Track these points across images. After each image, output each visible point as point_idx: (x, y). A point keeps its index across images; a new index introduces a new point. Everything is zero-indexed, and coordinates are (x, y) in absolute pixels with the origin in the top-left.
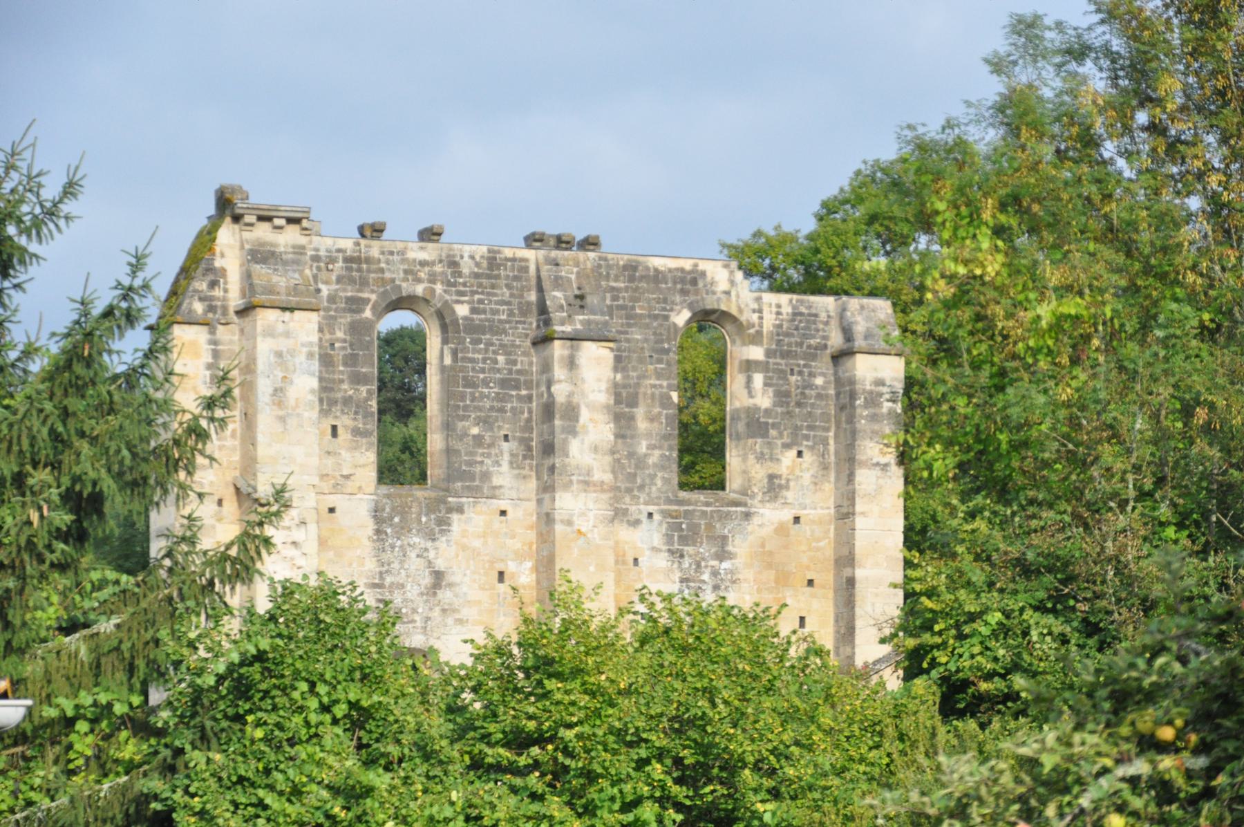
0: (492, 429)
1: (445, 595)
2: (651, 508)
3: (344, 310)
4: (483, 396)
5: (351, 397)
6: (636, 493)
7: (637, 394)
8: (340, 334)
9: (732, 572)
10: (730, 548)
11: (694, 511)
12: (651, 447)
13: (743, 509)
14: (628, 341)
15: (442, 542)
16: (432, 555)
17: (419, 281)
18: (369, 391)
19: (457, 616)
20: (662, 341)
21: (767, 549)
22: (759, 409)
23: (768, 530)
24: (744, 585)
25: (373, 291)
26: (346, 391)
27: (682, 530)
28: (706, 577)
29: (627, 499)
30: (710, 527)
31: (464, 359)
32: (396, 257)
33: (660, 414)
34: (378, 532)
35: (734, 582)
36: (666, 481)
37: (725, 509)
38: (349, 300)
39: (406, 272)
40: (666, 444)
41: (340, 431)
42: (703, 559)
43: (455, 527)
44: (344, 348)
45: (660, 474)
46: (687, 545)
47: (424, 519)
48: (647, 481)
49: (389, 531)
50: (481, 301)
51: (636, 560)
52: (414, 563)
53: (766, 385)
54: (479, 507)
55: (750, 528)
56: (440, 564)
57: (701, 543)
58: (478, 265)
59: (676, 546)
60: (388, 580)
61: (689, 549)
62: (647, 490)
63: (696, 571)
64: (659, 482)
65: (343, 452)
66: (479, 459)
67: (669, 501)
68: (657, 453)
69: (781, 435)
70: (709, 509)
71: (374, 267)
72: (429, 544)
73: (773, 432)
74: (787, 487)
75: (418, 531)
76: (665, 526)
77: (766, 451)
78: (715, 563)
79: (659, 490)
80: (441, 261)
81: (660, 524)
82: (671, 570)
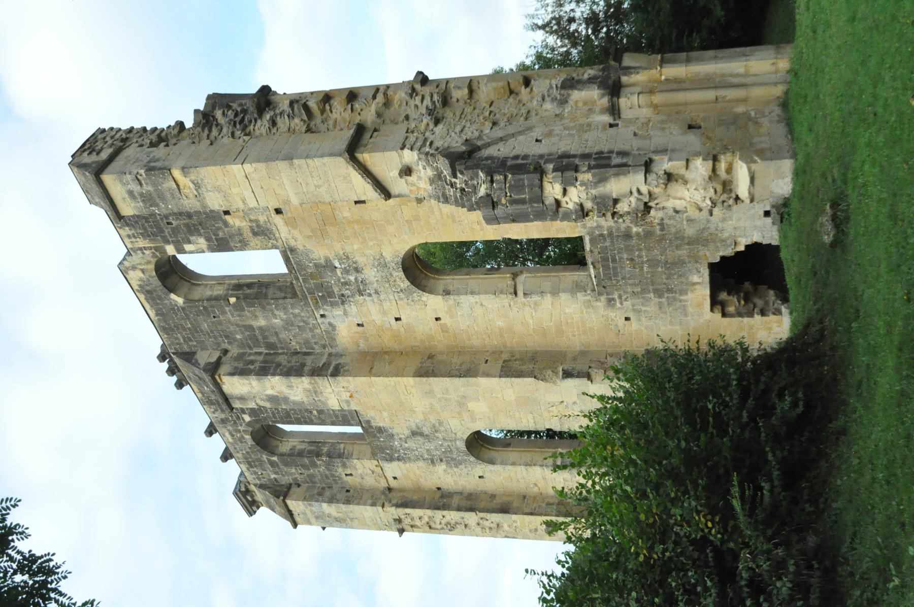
1: (426, 430)
2: (318, 316)
3: (279, 468)
6: (311, 326)
7: (245, 326)
9: (340, 260)
10: (322, 261)
12: (275, 316)
13: (289, 253)
14: (212, 332)
15: (395, 431)
16: (403, 436)
17: (242, 437)
18: (319, 460)
19: (437, 425)
20: (200, 311)
21: (311, 234)
22: (209, 245)
23: (296, 233)
24: (348, 249)
27: (323, 296)
28: (352, 278)
29: (318, 331)
30: (312, 276)
31: (275, 417)
32: (236, 446)
33: (249, 311)
34: (399, 459)
35: (348, 257)
36: (293, 306)
37: (295, 266)
39: (241, 442)
40: (268, 307)
42: (339, 280)
43: (381, 425)
45: (291, 311)
46: (334, 293)
48: (299, 318)
51: (358, 325)
53: (189, 242)
54: (363, 413)
55: (301, 248)
56: (407, 432)
57: (328, 282)
58: (216, 410)
59: (337, 299)
60: (426, 456)
61: (336, 290)
62: (305, 319)
64: (297, 311)
68: (277, 313)
69: (219, 229)
70: (300, 278)
72: (396, 437)
73: (221, 234)
74: (257, 221)
76: (325, 307)
77: (237, 240)
78: (339, 272)
79: (302, 310)
82: (356, 303)
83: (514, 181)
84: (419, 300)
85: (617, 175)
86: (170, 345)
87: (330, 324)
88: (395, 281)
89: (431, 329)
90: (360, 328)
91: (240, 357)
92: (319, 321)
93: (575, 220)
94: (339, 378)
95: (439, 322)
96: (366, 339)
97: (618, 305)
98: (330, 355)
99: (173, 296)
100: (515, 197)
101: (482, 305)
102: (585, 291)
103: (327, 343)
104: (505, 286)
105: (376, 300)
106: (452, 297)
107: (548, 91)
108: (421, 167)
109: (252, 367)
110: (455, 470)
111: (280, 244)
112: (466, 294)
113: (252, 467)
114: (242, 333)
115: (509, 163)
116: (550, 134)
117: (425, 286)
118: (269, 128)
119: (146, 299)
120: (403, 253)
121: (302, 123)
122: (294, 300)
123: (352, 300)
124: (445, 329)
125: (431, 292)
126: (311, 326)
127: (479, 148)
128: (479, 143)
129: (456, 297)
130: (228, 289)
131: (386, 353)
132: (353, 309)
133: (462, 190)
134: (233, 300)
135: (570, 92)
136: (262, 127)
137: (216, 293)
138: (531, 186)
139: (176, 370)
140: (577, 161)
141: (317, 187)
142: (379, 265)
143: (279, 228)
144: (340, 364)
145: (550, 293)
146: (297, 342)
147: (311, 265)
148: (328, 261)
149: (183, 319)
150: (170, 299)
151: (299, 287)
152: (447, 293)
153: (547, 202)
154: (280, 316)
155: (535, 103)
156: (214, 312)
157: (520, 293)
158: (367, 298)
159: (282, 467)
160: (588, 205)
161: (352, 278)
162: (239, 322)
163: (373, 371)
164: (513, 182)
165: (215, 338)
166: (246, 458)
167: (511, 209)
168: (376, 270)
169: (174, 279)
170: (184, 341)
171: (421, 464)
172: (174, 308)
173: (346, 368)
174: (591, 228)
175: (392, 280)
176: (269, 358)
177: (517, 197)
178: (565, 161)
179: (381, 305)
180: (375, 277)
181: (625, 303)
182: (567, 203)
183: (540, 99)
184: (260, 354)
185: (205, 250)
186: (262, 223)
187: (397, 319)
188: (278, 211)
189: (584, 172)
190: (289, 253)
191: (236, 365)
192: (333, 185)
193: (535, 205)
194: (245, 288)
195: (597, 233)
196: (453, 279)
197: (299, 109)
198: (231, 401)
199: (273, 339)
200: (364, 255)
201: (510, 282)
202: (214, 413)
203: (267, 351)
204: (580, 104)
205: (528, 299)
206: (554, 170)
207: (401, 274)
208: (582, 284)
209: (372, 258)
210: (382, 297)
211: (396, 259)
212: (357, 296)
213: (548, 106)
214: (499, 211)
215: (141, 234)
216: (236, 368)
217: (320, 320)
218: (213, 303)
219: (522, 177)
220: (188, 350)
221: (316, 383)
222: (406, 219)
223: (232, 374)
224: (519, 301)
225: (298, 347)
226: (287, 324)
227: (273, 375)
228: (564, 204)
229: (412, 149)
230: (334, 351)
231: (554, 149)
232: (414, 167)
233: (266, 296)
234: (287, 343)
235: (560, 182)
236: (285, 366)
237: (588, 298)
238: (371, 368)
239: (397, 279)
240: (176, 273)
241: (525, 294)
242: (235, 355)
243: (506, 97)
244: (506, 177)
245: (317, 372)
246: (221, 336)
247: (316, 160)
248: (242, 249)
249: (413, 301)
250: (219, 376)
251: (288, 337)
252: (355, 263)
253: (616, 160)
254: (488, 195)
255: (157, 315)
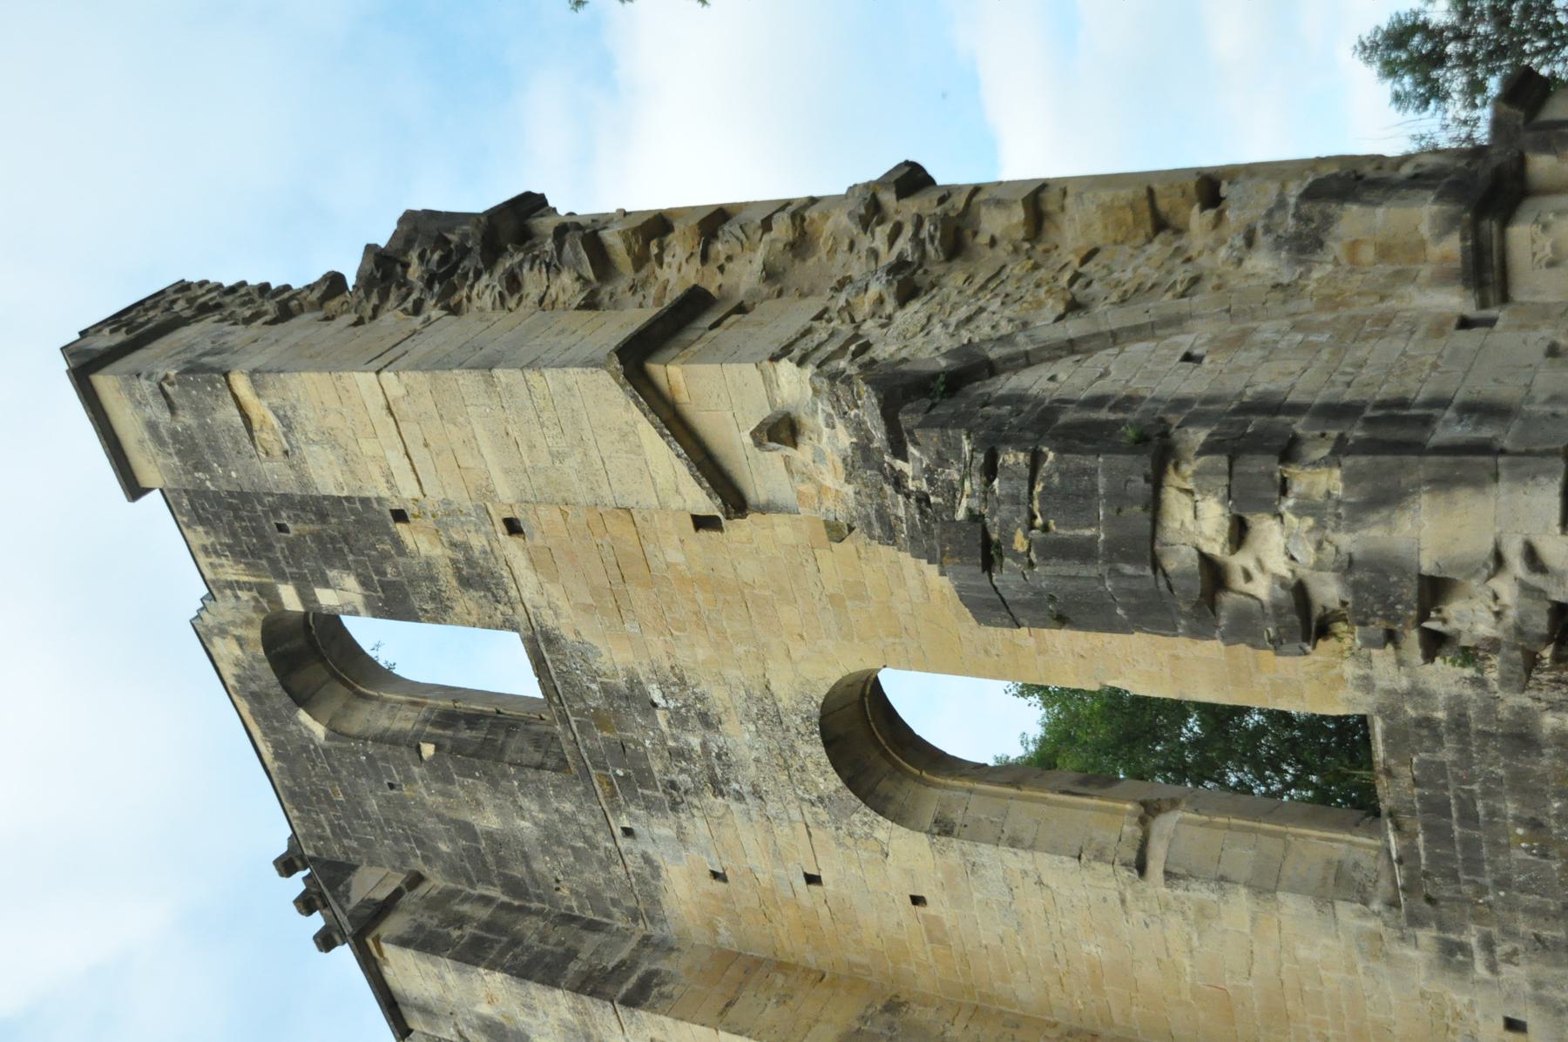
2: (618, 832)
6: (602, 854)
7: (454, 821)
9: (663, 684)
10: (621, 682)
11: (585, 747)
13: (542, 645)
14: (388, 821)
21: (590, 601)
23: (555, 591)
24: (683, 657)
27: (626, 777)
28: (695, 742)
29: (619, 870)
33: (462, 786)
35: (682, 682)
37: (558, 684)
42: (663, 742)
45: (556, 805)
46: (651, 773)
51: (715, 875)
53: (326, 584)
55: (571, 637)
57: (637, 743)
59: (660, 794)
61: (656, 766)
62: (588, 832)
63: (689, 760)
67: (590, 793)
68: (525, 802)
69: (385, 556)
70: (572, 719)
74: (465, 547)
81: (636, 819)
83: (1063, 474)
84: (868, 836)
85: (1443, 483)
86: (304, 836)
87: (647, 859)
88: (803, 769)
89: (899, 924)
90: (718, 886)
91: (438, 902)
92: (619, 843)
93: (1277, 644)
94: (642, 1014)
95: (920, 909)
96: (735, 919)
97: (1481, 970)
98: (646, 941)
99: (303, 716)
100: (1060, 531)
101: (1040, 883)
102: (1365, 902)
103: (641, 907)
104: (1114, 837)
105: (755, 816)
106: (955, 843)
107: (1270, 214)
108: (820, 419)
109: (455, 933)
111: (520, 617)
112: (997, 842)
114: (452, 840)
115: (1068, 416)
116: (1240, 340)
117: (888, 799)
118: (501, 294)
119: (252, 713)
120: (825, 691)
121: (577, 286)
122: (560, 776)
123: (696, 802)
124: (936, 934)
125: (899, 818)
126: (602, 854)
127: (991, 369)
128: (994, 353)
129: (967, 846)
130: (426, 721)
131: (781, 967)
132: (698, 828)
133: (923, 499)
134: (428, 750)
135: (1333, 208)
136: (488, 292)
137: (398, 725)
138: (1118, 498)
139: (319, 903)
140: (1299, 426)
141: (557, 456)
142: (760, 715)
143: (516, 573)
144: (656, 973)
145: (1248, 885)
146: (571, 890)
147: (594, 687)
148: (634, 682)
149: (327, 777)
150: (298, 723)
151: (569, 742)
152: (944, 828)
153: (1171, 564)
154: (530, 811)
155: (1223, 252)
156: (391, 776)
157: (1155, 867)
158: (734, 806)
160: (1329, 592)
161: (695, 742)
162: (442, 810)
163: (732, 1013)
164: (1056, 480)
165: (396, 840)
167: (1045, 574)
168: (753, 728)
169: (313, 673)
170: (333, 832)
172: (306, 745)
173: (666, 989)
174: (1391, 692)
175: (796, 763)
176: (505, 918)
177: (1065, 533)
178: (1256, 422)
179: (770, 831)
180: (751, 748)
181: (1504, 968)
182: (1248, 577)
183: (1239, 242)
184: (486, 901)
185: (361, 608)
186: (477, 553)
187: (812, 879)
188: (513, 527)
189: (1315, 464)
190: (542, 645)
191: (425, 919)
192: (594, 454)
193: (1128, 569)
194: (462, 724)
195: (1412, 713)
196: (970, 791)
197: (574, 247)
198: (404, 1010)
199: (518, 871)
200: (722, 680)
201: (1131, 829)
203: (505, 899)
204: (1368, 254)
205: (1179, 892)
206: (1208, 449)
207: (819, 752)
208: (1358, 876)
209: (742, 693)
210: (773, 808)
211: (804, 707)
212: (709, 795)
213: (1263, 263)
214: (1008, 577)
215: (229, 547)
216: (420, 928)
217: (624, 843)
218: (386, 748)
219: (1088, 461)
220: (342, 858)
221: (587, 1012)
222: (830, 590)
223: (403, 942)
224: (1150, 891)
225: (574, 904)
226: (548, 837)
227: (492, 966)
228: (1238, 582)
229: (801, 363)
230: (656, 932)
231: (1233, 385)
232: (806, 420)
233: (498, 753)
234: (549, 886)
235: (1223, 492)
236: (528, 948)
237: (1373, 924)
238: (729, 1005)
239: (810, 766)
240: (323, 660)
241: (1169, 875)
242: (434, 893)
243: (1140, 240)
244: (1036, 460)
245: (594, 985)
246: (408, 840)
247: (548, 373)
248: (438, 618)
249: (851, 835)
250: (377, 940)
252: (701, 699)
253: (1451, 430)
254: (974, 517)
255: (277, 756)
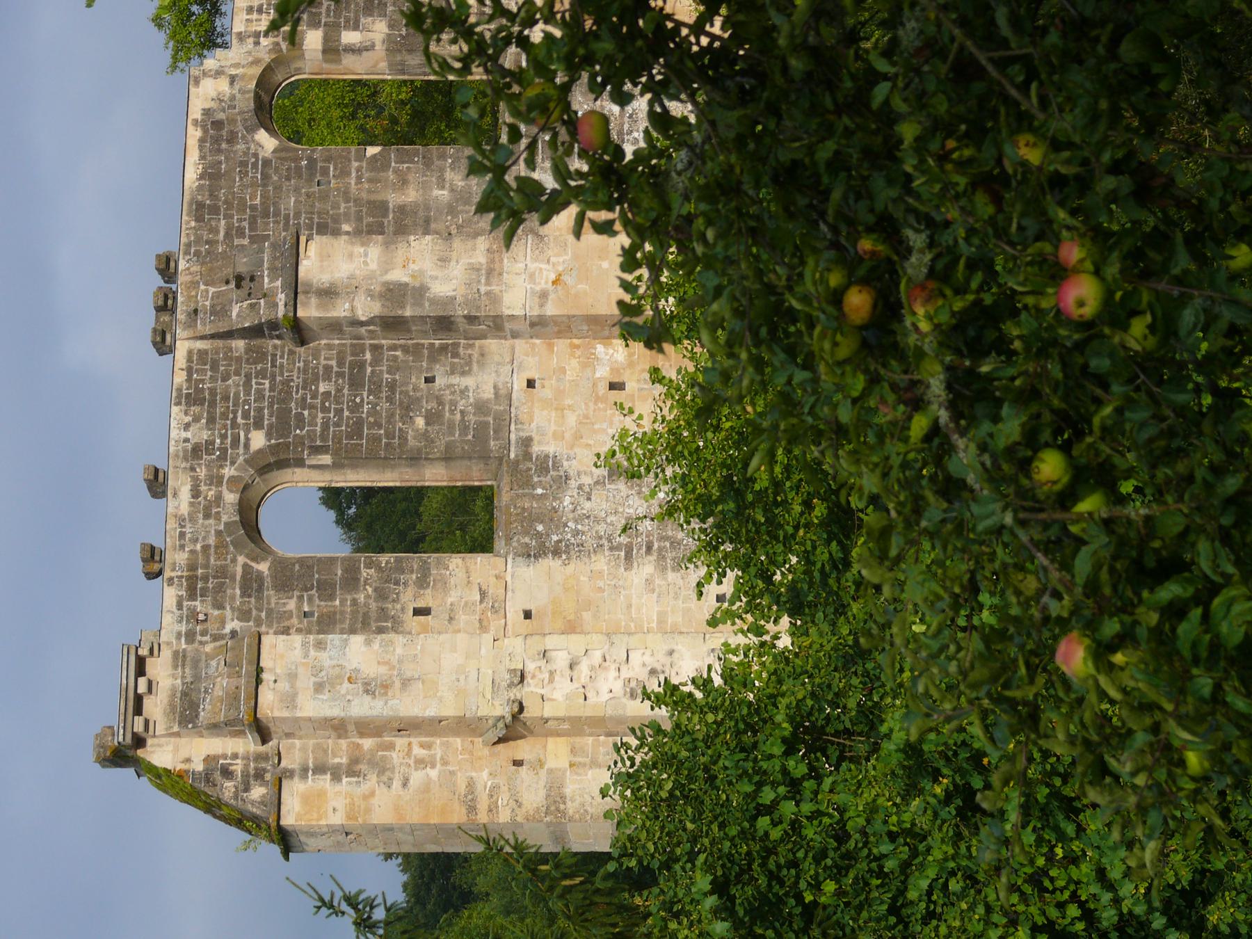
0: (419, 400)
4: (373, 412)
5: (375, 590)
7: (369, 202)
8: (292, 605)
16: (587, 480)
17: (219, 498)
18: (368, 566)
20: (298, 168)
25: (234, 561)
26: (368, 597)
31: (324, 437)
32: (188, 530)
33: (396, 171)
34: (556, 553)
38: (243, 595)
41: (421, 604)
43: (551, 449)
44: (310, 599)
47: (539, 491)
49: (555, 538)
50: (246, 415)
52: (598, 504)
54: (523, 417)
58: (196, 419)
65: (450, 600)
66: (458, 417)
68: (449, 175)
71: (201, 560)
72: (573, 484)
75: (555, 499)
80: (193, 469)
99: (262, 136)
110: (671, 576)
113: (192, 595)
119: (202, 141)
159: (269, 593)
162: (364, 195)
166: (192, 567)
170: (227, 235)
171: (601, 562)
202: (187, 427)
251: (447, 227)
